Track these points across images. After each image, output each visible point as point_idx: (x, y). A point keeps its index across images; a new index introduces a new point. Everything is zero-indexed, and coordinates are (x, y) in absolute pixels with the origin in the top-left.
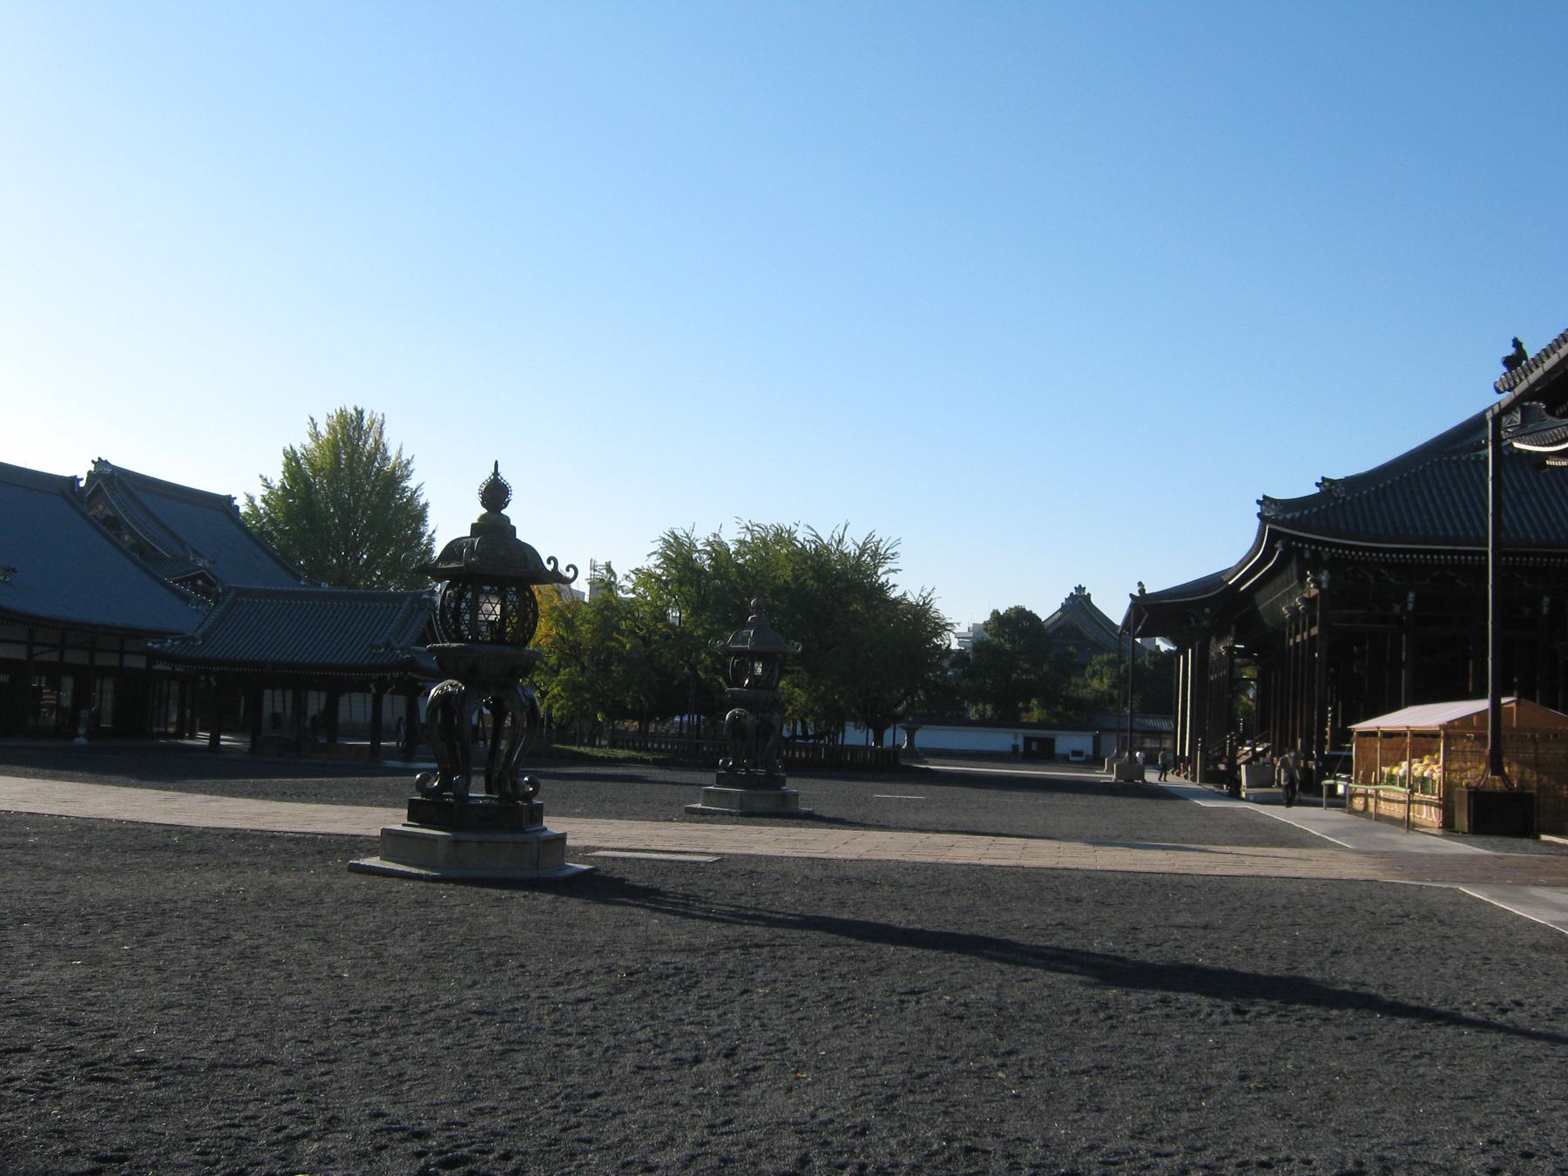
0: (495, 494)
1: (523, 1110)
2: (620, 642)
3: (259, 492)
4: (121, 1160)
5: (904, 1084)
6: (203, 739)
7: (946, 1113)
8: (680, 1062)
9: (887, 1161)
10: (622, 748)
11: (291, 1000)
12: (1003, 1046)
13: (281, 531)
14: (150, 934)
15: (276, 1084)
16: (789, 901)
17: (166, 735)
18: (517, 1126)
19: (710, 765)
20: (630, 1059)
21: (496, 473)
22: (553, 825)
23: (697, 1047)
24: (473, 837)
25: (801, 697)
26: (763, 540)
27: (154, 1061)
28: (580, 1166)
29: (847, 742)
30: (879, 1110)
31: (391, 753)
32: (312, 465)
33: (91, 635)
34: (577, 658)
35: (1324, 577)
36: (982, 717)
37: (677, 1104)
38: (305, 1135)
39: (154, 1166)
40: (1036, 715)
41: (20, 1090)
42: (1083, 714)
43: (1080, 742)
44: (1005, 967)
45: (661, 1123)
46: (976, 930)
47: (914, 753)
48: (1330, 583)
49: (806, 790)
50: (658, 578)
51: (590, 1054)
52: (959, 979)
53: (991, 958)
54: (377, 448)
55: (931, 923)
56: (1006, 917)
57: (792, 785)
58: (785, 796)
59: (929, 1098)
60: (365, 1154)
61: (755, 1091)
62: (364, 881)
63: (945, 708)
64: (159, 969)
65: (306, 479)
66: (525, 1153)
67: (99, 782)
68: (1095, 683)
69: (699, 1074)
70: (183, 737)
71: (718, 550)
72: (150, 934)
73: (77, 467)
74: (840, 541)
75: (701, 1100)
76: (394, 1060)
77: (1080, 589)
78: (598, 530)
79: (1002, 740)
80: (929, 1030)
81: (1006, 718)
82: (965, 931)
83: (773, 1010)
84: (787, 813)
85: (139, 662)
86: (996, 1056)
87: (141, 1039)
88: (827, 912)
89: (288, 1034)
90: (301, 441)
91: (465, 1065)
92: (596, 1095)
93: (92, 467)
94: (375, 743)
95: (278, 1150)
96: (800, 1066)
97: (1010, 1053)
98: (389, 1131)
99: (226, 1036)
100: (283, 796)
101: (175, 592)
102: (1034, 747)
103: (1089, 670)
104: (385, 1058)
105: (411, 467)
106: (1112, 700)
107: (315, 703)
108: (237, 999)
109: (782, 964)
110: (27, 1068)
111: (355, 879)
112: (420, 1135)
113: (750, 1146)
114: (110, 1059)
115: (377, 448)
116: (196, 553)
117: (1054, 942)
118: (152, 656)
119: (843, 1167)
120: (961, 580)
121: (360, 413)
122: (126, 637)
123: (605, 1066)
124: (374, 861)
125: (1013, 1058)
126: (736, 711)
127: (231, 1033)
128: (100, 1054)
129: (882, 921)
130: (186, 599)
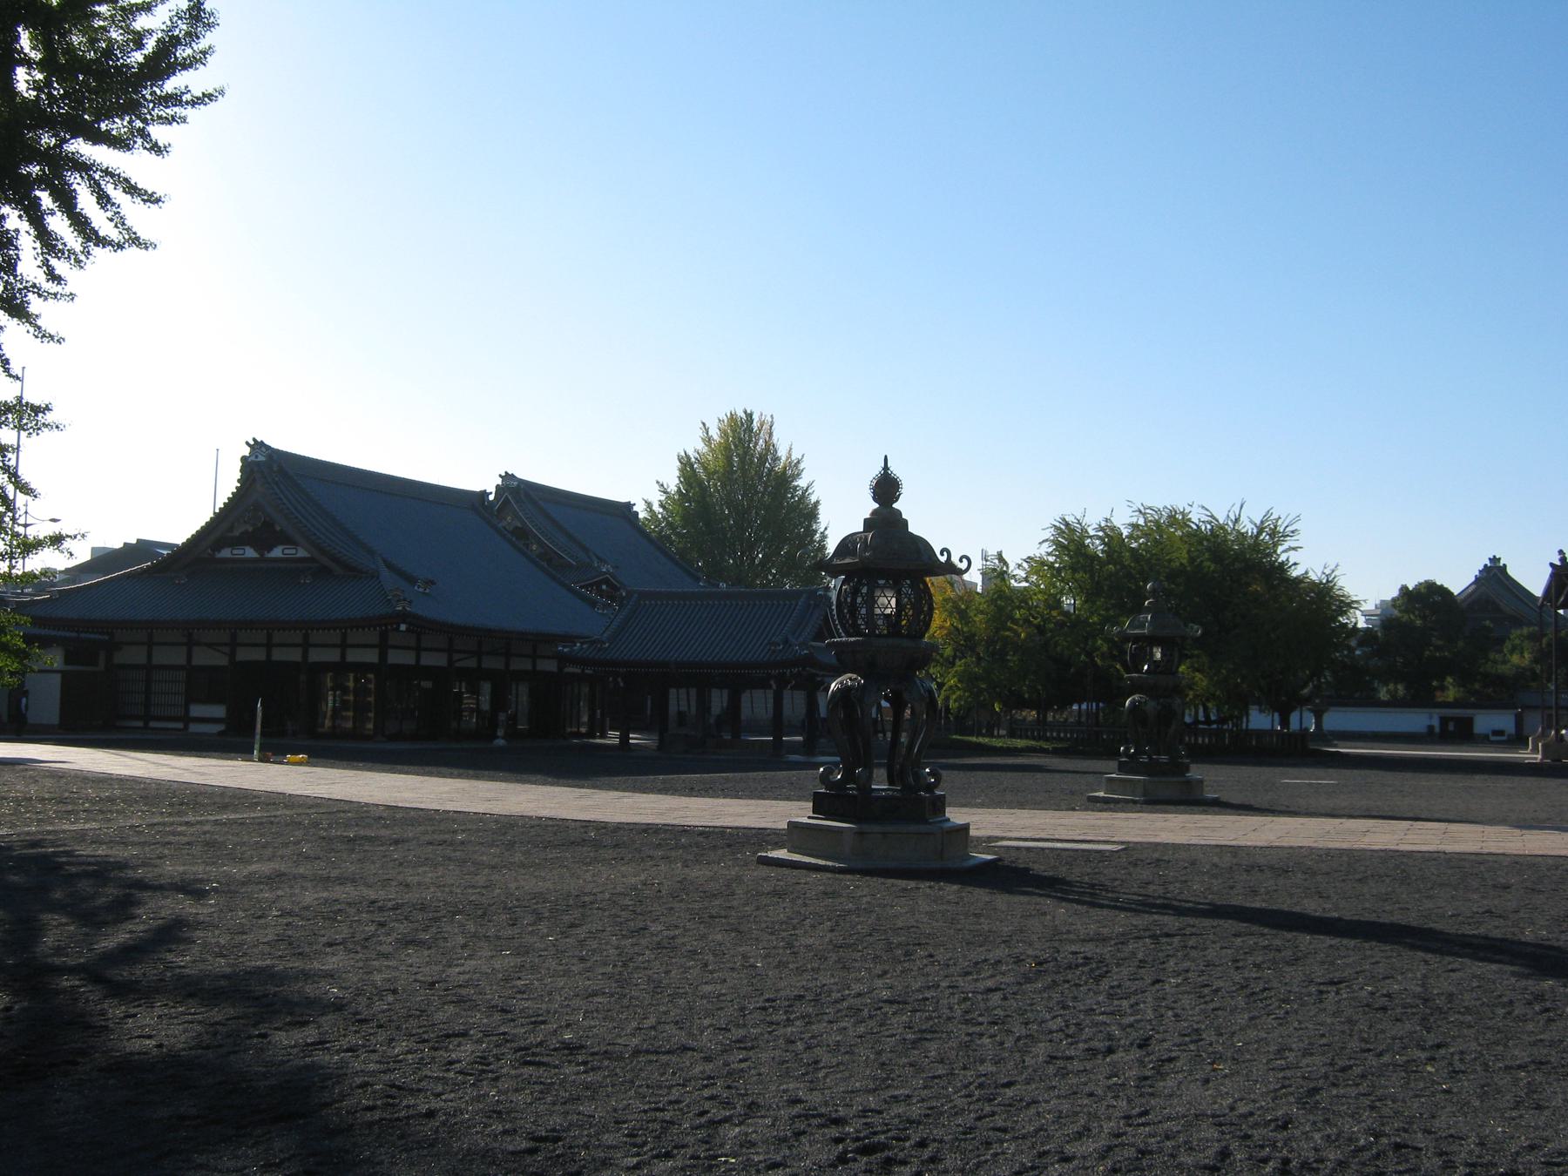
0: (886, 488)
1: (937, 1098)
2: (1015, 632)
3: (656, 498)
4: (556, 1140)
5: (1326, 1077)
6: (613, 738)
7: (1372, 1108)
8: (1092, 1053)
9: (1311, 1155)
10: (1021, 737)
11: (708, 988)
12: (1431, 1039)
13: (678, 535)
14: (572, 926)
15: (697, 1070)
16: (1198, 889)
17: (578, 735)
18: (933, 1114)
19: (1113, 754)
20: (1041, 1049)
21: (886, 468)
22: (956, 815)
23: (1110, 1037)
24: (876, 828)
26: (1157, 522)
27: (582, 1047)
28: (996, 1155)
29: (1252, 726)
30: (1302, 1104)
31: (793, 748)
32: (705, 469)
34: (972, 649)
36: (1393, 694)
37: (1091, 1095)
38: (726, 1120)
39: (586, 1147)
40: (1452, 694)
41: (460, 1072)
42: (1503, 691)
43: (1504, 721)
44: (1429, 956)
45: (1076, 1114)
46: (1397, 918)
47: (1323, 736)
49: (1211, 777)
50: (1051, 566)
51: (1002, 1043)
52: (1381, 970)
53: (1413, 947)
55: (1348, 911)
56: (1429, 904)
57: (1196, 772)
58: (1188, 782)
59: (1353, 1091)
60: (785, 1139)
61: (1170, 1083)
62: (774, 873)
63: (1354, 688)
64: (582, 959)
65: (700, 483)
66: (941, 1141)
67: (518, 781)
68: (1515, 659)
69: (1113, 1064)
70: (591, 735)
71: (1111, 535)
72: (572, 926)
73: (484, 481)
74: (1237, 520)
75: (1116, 1091)
76: (809, 1048)
77: (1495, 560)
78: (990, 521)
79: (1417, 720)
80: (1350, 1021)
81: (1420, 697)
82: (1385, 919)
83: (1186, 1001)
84: (1192, 800)
85: (550, 666)
86: (1424, 1049)
87: (568, 1026)
88: (1238, 901)
89: (706, 1022)
90: (694, 445)
91: (879, 1053)
92: (1009, 1085)
93: (499, 481)
94: (778, 739)
95: (701, 1134)
96: (1217, 1058)
97: (1439, 1046)
98: (807, 1117)
99: (648, 1023)
100: (691, 791)
102: (1451, 727)
103: (1508, 644)
104: (800, 1046)
105: (801, 466)
106: (1535, 677)
107: (718, 700)
108: (657, 988)
109: (1194, 953)
110: (465, 1052)
111: (764, 871)
112: (837, 1122)
113: (1168, 1138)
114: (540, 1044)
115: (767, 449)
116: (600, 560)
117: (1482, 931)
118: (563, 659)
119: (1265, 1161)
120: (1367, 552)
121: (750, 416)
122: (539, 642)
123: (1017, 1055)
124: (782, 854)
125: (1442, 1051)
126: (1136, 697)
127: (652, 1021)
128: (531, 1039)
129: (1297, 909)
130: (593, 604)
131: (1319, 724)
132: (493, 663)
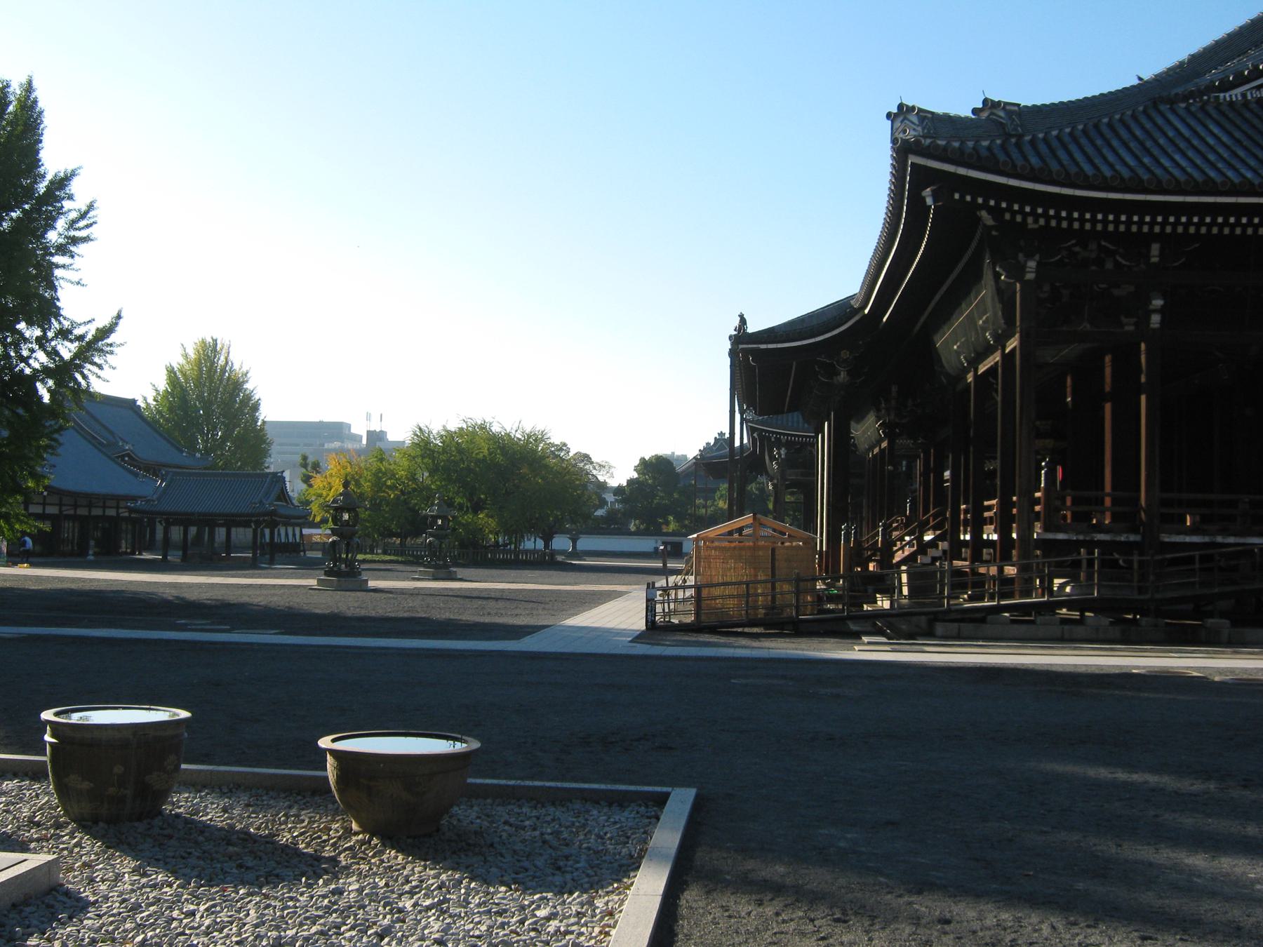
13: (167, 420)
17: (126, 553)
25: (493, 523)
32: (184, 375)
33: (91, 499)
35: (783, 451)
40: (672, 526)
47: (576, 554)
54: (227, 363)
63: (613, 525)
65: (181, 387)
79: (647, 544)
81: (651, 529)
85: (111, 512)
90: (177, 361)
107: (193, 530)
115: (227, 363)
118: (131, 510)
121: (215, 341)
122: (104, 500)
130: (136, 475)
131: (574, 547)
132: (82, 512)
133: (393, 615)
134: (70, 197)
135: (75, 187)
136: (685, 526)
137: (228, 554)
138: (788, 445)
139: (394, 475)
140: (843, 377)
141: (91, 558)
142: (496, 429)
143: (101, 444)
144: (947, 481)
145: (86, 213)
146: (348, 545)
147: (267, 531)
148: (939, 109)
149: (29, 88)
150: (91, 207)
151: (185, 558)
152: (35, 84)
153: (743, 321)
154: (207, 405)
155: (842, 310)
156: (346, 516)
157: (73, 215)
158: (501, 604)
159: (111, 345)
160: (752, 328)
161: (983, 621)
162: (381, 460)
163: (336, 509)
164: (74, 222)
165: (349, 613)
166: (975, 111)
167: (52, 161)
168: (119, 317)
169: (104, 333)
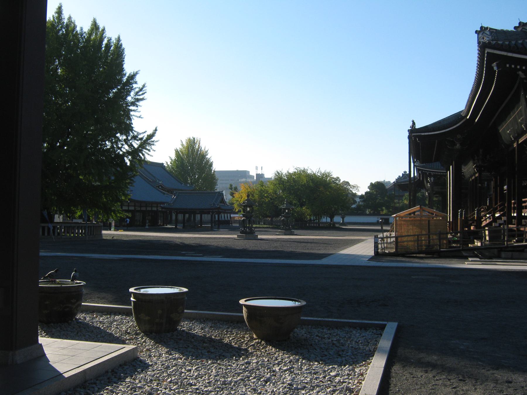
13: (175, 171)
17: (161, 225)
25: (309, 211)
32: (182, 153)
33: (147, 204)
35: (432, 179)
40: (385, 212)
47: (344, 224)
48: (434, 180)
54: (199, 147)
63: (359, 211)
79: (374, 219)
81: (376, 213)
90: (179, 147)
101: (161, 192)
103: (404, 197)
107: (187, 216)
116: (159, 180)
118: (162, 208)
121: (194, 139)
122: (152, 204)
130: (164, 194)
132: (143, 209)
133: (268, 249)
134: (136, 83)
135: (137, 78)
136: (390, 212)
137: (201, 225)
138: (435, 176)
139: (267, 192)
140: (458, 146)
141: (147, 227)
142: (309, 172)
143: (150, 181)
144: (505, 190)
145: (142, 89)
146: (249, 221)
147: (217, 216)
148: (499, 27)
149: (119, 40)
150: (144, 86)
151: (184, 227)
152: (121, 38)
153: (414, 123)
154: (192, 165)
155: (457, 117)
156: (248, 209)
157: (137, 90)
158: (313, 245)
159: (153, 142)
160: (417, 126)
161: (523, 251)
162: (262, 186)
163: (244, 206)
164: (137, 93)
165: (251, 249)
166: (515, 28)
167: (128, 68)
168: (156, 130)
169: (151, 136)
